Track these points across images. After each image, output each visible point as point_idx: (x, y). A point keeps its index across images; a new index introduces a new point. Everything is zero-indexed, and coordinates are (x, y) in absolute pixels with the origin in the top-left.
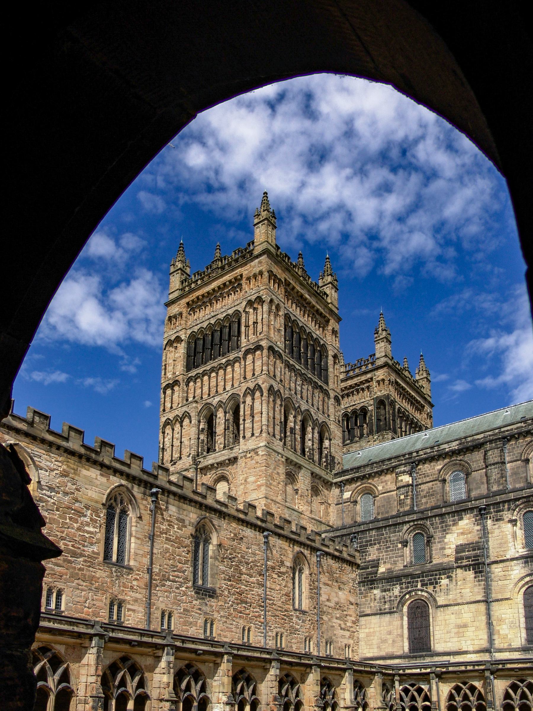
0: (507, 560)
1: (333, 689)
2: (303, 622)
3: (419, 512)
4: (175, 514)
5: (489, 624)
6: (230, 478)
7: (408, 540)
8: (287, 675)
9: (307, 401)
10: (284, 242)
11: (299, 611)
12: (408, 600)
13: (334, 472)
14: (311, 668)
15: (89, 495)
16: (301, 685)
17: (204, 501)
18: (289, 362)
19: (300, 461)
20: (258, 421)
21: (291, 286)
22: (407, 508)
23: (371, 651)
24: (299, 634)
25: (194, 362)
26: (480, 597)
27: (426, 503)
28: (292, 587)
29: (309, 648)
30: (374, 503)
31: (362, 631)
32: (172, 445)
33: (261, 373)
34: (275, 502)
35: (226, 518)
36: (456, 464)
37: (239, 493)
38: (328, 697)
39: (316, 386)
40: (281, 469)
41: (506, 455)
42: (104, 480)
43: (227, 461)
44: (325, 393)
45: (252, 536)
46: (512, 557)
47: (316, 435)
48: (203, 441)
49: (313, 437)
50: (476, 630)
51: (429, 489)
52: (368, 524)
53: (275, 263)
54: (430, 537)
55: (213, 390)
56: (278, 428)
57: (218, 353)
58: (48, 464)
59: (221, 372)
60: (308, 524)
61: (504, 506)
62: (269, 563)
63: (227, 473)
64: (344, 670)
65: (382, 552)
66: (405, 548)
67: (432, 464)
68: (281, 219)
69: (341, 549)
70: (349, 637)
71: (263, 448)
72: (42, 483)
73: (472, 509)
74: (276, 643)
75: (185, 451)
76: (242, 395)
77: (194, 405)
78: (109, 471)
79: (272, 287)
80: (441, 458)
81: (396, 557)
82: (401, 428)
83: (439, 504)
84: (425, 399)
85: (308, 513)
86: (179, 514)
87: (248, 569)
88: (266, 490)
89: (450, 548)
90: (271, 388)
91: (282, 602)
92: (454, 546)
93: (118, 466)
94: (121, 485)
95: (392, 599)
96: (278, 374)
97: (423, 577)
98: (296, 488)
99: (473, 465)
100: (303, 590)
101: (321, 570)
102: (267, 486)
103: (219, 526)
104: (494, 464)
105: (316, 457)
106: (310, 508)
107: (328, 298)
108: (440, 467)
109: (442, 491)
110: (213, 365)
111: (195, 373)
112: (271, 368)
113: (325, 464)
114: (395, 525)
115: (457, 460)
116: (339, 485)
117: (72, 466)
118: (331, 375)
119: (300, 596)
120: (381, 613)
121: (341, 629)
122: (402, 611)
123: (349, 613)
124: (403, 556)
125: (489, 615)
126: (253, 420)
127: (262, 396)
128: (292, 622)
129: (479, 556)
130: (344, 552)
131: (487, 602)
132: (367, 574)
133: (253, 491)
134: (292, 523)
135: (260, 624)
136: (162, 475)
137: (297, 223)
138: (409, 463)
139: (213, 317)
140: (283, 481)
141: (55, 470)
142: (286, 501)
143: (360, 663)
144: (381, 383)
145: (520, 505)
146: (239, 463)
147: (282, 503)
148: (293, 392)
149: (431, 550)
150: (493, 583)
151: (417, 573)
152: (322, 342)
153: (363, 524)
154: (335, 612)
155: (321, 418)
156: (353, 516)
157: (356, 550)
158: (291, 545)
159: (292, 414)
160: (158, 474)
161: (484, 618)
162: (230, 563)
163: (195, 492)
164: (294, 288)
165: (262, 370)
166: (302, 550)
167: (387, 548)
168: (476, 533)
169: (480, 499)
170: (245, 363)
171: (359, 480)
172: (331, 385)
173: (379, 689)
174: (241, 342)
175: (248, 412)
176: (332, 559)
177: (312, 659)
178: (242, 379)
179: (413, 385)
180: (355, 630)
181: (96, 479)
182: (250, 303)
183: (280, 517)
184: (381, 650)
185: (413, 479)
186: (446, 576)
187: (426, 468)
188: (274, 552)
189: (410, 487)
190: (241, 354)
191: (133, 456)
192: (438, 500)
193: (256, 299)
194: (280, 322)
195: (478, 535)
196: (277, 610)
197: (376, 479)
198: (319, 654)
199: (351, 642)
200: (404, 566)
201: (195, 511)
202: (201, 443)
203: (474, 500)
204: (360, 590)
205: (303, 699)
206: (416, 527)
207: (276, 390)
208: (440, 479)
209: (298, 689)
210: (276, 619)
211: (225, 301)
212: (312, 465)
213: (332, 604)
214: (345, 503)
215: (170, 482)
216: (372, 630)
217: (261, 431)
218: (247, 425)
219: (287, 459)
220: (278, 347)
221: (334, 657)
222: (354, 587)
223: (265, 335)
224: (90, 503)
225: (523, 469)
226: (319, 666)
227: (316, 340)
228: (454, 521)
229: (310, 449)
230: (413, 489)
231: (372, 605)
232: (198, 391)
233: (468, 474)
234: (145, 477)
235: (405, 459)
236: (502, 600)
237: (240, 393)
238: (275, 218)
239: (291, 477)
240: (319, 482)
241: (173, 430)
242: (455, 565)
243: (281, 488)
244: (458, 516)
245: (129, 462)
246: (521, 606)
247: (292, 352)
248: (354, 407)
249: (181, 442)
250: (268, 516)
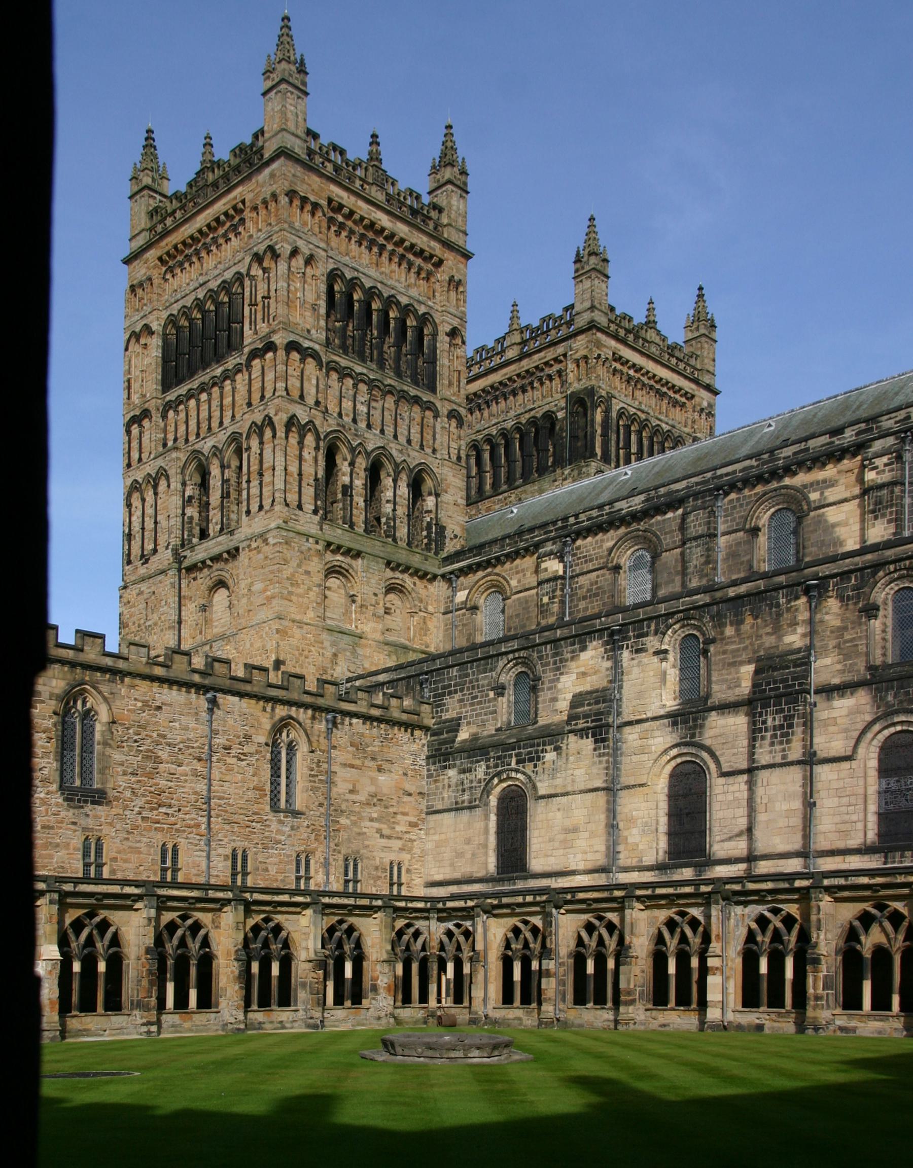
65: (465, 706)
66: (500, 699)
81: (486, 714)
89: (565, 699)
92: (569, 696)
124: (495, 712)
125: (612, 812)
149: (537, 703)
153: (440, 656)
167: (473, 698)
168: (604, 672)
195: (607, 676)
228: (573, 652)
242: (568, 728)
244: (580, 642)
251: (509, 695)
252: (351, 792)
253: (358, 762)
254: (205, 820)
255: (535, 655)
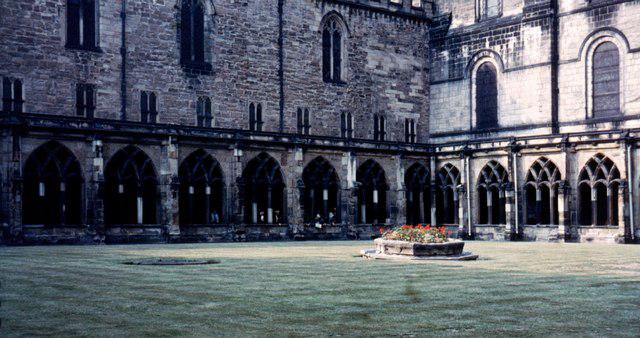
131: (555, 62)
252: (378, 67)
253: (382, 46)
254: (279, 86)
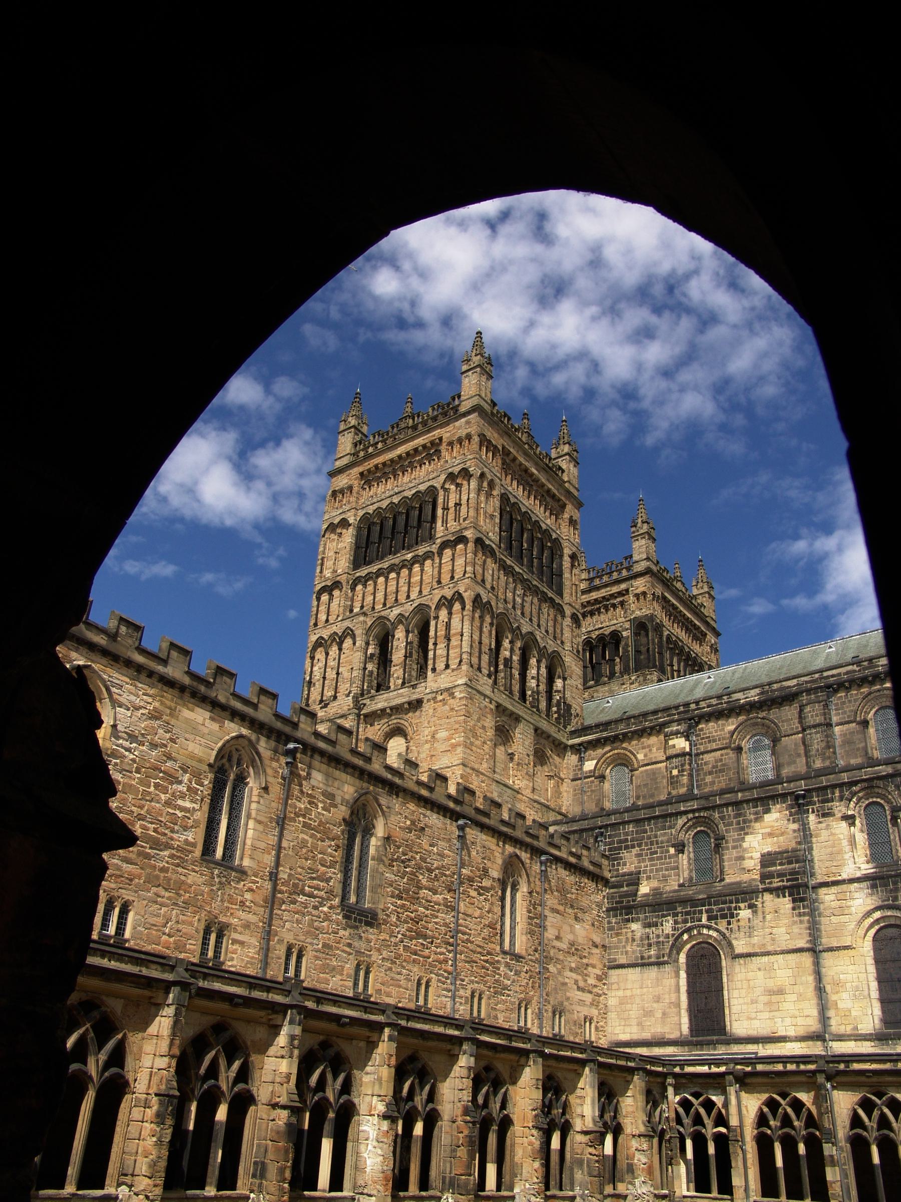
0: (843, 882)
1: (564, 1097)
2: (516, 974)
3: (701, 798)
4: (321, 785)
5: (820, 990)
6: (409, 730)
7: (686, 842)
8: (488, 1069)
9: (531, 620)
10: (502, 397)
11: (511, 954)
12: (687, 942)
13: (570, 728)
14: (528, 1057)
15: (190, 749)
16: (510, 1088)
17: (368, 767)
18: (505, 562)
19: (519, 710)
20: (456, 647)
21: (511, 457)
22: (683, 790)
23: (628, 1029)
24: (508, 995)
25: (365, 556)
26: (802, 943)
27: (712, 783)
28: (500, 913)
29: (526, 1021)
30: (632, 780)
31: (613, 994)
32: (324, 678)
33: (464, 575)
34: (478, 772)
35: (401, 794)
36: (756, 724)
37: (423, 756)
38: (556, 1111)
39: (544, 598)
40: (488, 720)
41: (833, 713)
42: (215, 726)
43: (406, 706)
44: (558, 610)
45: (440, 825)
46: (851, 877)
47: (543, 671)
48: (371, 672)
49: (538, 673)
50: (798, 1000)
51: (716, 761)
52: (622, 813)
53: (489, 424)
54: (720, 839)
55: (391, 598)
56: (485, 658)
57: (401, 545)
58: (133, 698)
59: (405, 572)
60: (528, 809)
61: (833, 793)
62: (464, 871)
63: (405, 723)
64: (583, 1063)
65: (644, 861)
66: (680, 855)
67: (720, 722)
68: (500, 367)
69: (579, 853)
70: (592, 1004)
71: (462, 688)
72: (119, 728)
73: (784, 796)
74: (472, 1010)
75: (343, 688)
76: (433, 607)
77: (362, 618)
78: (223, 714)
79: (484, 457)
80: (734, 714)
81: (667, 870)
82: (672, 665)
83: (732, 785)
84: (707, 624)
85: (527, 792)
86: (327, 785)
87: (430, 880)
88: (465, 753)
89: (751, 858)
90: (477, 599)
91: (483, 938)
92: (757, 855)
93: (238, 705)
94: (240, 736)
95: (661, 939)
96: (488, 578)
97: (710, 904)
98: (510, 751)
99: (783, 726)
100: (518, 919)
101: (547, 886)
102: (466, 746)
103: (388, 807)
104: (814, 726)
105: (543, 705)
106: (531, 784)
107: (565, 474)
108: (732, 727)
109: (736, 765)
110: (392, 562)
111: (366, 572)
112: (479, 569)
113: (556, 716)
114: (664, 816)
115: (758, 718)
116: (578, 749)
117: (168, 703)
118: (567, 583)
119: (513, 928)
120: (643, 964)
121: (579, 988)
122: (677, 961)
123: (591, 961)
124: (677, 868)
126: (448, 645)
127: (463, 609)
128: (498, 974)
129: (797, 873)
130: (583, 858)
131: (815, 950)
132: (620, 897)
133: (444, 754)
134: (504, 807)
135: (446, 974)
136: (306, 723)
137: (522, 373)
138: (684, 719)
139: (396, 494)
140: (491, 740)
141: (141, 708)
142: (494, 771)
143: (609, 1052)
144: (642, 597)
145: (859, 792)
146: (424, 709)
147: (488, 774)
148: (510, 606)
149: (722, 861)
150: (822, 919)
151: (701, 897)
152: (554, 536)
153: (615, 812)
154: (569, 959)
155: (551, 646)
156: (599, 800)
157: (604, 856)
158: (501, 844)
159: (507, 638)
160: (299, 721)
161: (810, 979)
162: (402, 869)
163: (354, 752)
164: (515, 459)
165: (465, 572)
166: (518, 852)
167: (652, 853)
168: (791, 835)
169: (797, 780)
170: (441, 560)
171: (608, 742)
172: (567, 598)
173: (641, 1099)
174: (435, 531)
175: (442, 633)
176: (565, 869)
177: (530, 1040)
178: (434, 583)
179: (689, 602)
180: (601, 992)
181: (203, 725)
182: (451, 477)
183: (485, 797)
184: (643, 1029)
185: (690, 745)
186: (746, 904)
187: (710, 728)
188: (474, 853)
189: (687, 757)
190: (434, 548)
191: (263, 691)
192: (730, 779)
193: (460, 472)
194: (494, 504)
195: (795, 837)
196: (474, 952)
197: (634, 742)
198: (541, 1031)
199: (594, 1012)
200: (680, 885)
201: (351, 782)
202: (369, 676)
203: (789, 782)
204: (609, 923)
205: (513, 1113)
206: (698, 821)
207: (484, 601)
208: (733, 746)
209: (505, 1094)
210: (472, 967)
211: (416, 473)
212: (536, 717)
213: (564, 946)
214: (586, 778)
215: (317, 735)
216: (628, 993)
217: (461, 661)
218: (439, 652)
219: (498, 706)
220: (490, 540)
221: (566, 1038)
222: (599, 916)
223: (471, 522)
224: (190, 762)
225: (860, 736)
226: (541, 1054)
227: (546, 533)
228: (756, 813)
229: (533, 692)
230: (691, 760)
231: (629, 948)
232: (369, 599)
233: (775, 741)
234: (279, 725)
235: (678, 713)
236: (838, 949)
237: (430, 604)
238: (492, 366)
239: (503, 734)
240: (546, 742)
241: (327, 654)
243: (487, 751)
245: (256, 701)
246: (870, 961)
247: (510, 547)
248: (601, 631)
249: (338, 674)
250: (466, 795)
251: (689, 852)
255: (717, 815)
